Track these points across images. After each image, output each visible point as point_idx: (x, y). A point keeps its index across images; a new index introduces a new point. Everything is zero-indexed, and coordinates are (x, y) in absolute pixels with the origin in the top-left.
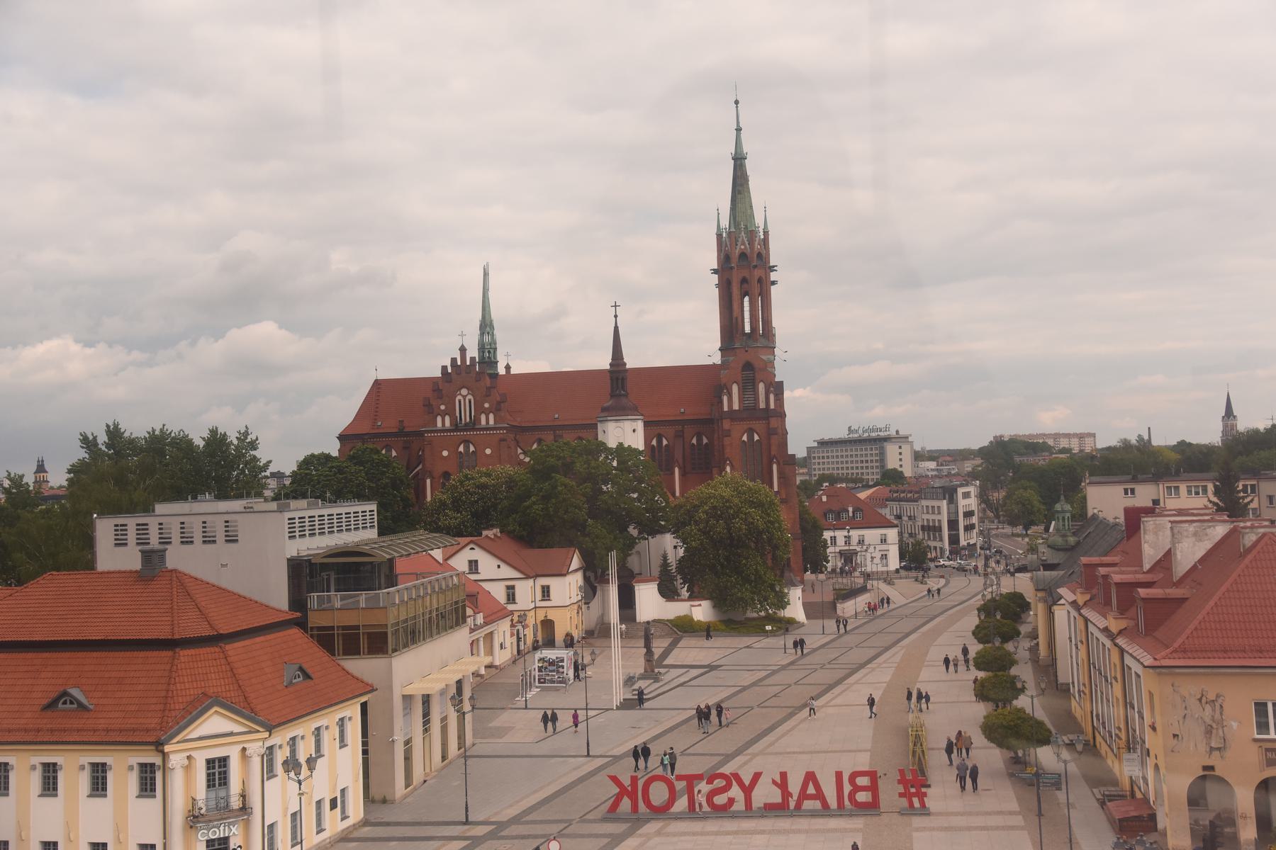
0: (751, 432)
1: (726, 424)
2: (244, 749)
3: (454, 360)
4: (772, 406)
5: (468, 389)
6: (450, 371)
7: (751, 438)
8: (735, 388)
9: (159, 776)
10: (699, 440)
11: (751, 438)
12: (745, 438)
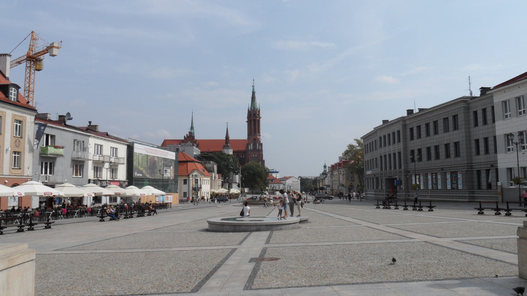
0: (255, 154)
1: (249, 152)
2: (200, 178)
3: (187, 135)
4: (260, 149)
5: (190, 141)
6: (186, 137)
7: (255, 156)
8: (252, 144)
9: (187, 181)
10: (242, 156)
11: (255, 156)
12: (253, 156)
